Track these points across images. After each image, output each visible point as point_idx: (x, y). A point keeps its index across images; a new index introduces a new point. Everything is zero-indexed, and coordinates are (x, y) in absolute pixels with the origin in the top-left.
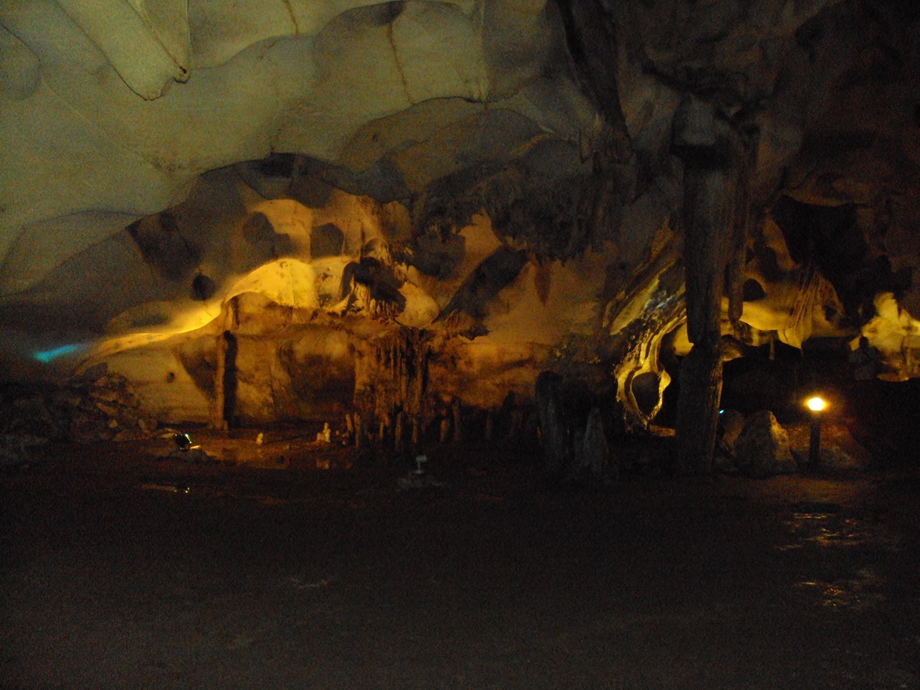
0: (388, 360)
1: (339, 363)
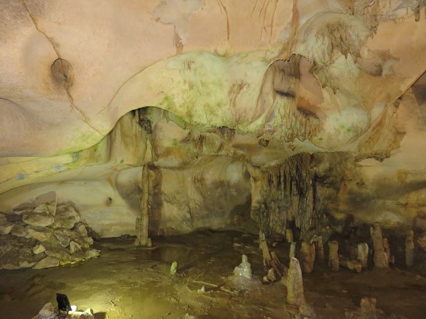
0: (279, 183)
1: (237, 187)
